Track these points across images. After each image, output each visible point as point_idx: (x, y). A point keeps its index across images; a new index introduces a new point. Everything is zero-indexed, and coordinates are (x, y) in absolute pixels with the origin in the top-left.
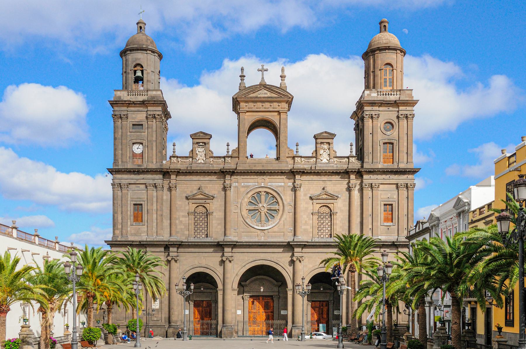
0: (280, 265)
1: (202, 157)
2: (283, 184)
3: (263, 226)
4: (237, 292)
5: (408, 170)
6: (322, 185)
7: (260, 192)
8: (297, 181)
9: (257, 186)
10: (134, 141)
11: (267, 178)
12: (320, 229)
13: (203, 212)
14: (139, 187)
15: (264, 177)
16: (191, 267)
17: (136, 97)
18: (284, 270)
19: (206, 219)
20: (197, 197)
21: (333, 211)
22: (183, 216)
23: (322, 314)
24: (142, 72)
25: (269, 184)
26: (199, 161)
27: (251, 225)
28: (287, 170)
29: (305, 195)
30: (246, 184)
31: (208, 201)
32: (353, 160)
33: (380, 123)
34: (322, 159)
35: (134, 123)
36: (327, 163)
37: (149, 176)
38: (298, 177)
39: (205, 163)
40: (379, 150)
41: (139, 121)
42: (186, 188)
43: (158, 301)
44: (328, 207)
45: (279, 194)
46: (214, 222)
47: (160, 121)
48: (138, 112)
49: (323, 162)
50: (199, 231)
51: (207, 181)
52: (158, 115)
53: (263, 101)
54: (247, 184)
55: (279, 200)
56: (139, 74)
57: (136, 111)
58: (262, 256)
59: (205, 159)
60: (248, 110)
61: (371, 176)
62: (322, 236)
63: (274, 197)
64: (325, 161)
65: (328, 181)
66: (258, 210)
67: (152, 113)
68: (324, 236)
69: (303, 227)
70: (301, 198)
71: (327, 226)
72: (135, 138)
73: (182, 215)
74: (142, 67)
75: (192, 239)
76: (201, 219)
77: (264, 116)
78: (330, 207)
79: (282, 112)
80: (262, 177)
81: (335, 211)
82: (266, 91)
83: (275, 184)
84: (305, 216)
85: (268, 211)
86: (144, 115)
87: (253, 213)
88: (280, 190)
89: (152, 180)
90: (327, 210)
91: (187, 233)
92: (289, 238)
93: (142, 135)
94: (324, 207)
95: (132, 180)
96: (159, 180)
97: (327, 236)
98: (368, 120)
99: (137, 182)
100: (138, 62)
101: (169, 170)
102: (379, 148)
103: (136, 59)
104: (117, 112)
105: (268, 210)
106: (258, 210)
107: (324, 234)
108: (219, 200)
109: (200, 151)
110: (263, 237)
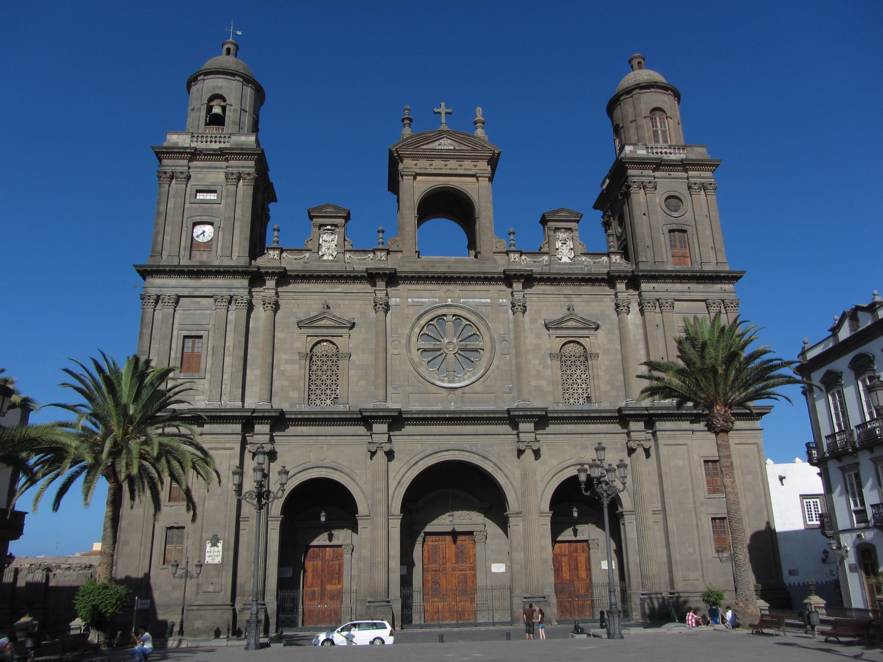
0: (491, 461)
1: (330, 251)
2: (489, 301)
3: (453, 382)
4: (400, 521)
5: (722, 274)
6: (563, 302)
7: (445, 315)
8: (517, 293)
9: (438, 305)
10: (197, 219)
11: (455, 289)
12: (566, 386)
13: (330, 355)
14: (199, 303)
15: (452, 287)
16: (300, 468)
17: (208, 145)
18: (500, 472)
19: (334, 368)
20: (319, 323)
21: (589, 352)
22: (288, 362)
23: (577, 568)
24: (224, 109)
25: (462, 300)
26: (325, 258)
27: (428, 378)
28: (497, 273)
29: (533, 321)
30: (416, 300)
31: (340, 331)
32: (616, 258)
33: (658, 198)
34: (560, 257)
35: (201, 188)
36: (570, 264)
37: (220, 281)
38: (517, 286)
39: (337, 261)
40: (663, 242)
41: (210, 184)
42: (296, 306)
43: (220, 545)
44: (578, 343)
45: (482, 319)
46: (352, 372)
47: (249, 184)
48: (212, 170)
49: (562, 261)
50: (318, 392)
51: (337, 294)
52: (249, 174)
53: (445, 157)
54: (419, 300)
55: (483, 329)
56: (217, 110)
57: (205, 168)
58: (453, 441)
59: (336, 253)
60: (418, 171)
61: (656, 285)
62: (572, 401)
63: (471, 324)
64: (565, 259)
65: (575, 296)
66: (439, 350)
67: (236, 170)
68: (576, 401)
69: (533, 383)
70: (527, 326)
71: (579, 381)
72: (200, 214)
73: (286, 360)
74: (224, 100)
75: (304, 408)
76: (325, 368)
77: (450, 183)
78: (583, 343)
79: (480, 177)
80: (445, 287)
81: (593, 351)
82: (449, 141)
83: (474, 300)
84: (535, 362)
85: (459, 352)
86: (222, 176)
87: (430, 356)
88: (484, 311)
89: (225, 290)
90: (577, 349)
91: (294, 395)
92: (507, 403)
93: (214, 209)
94: (572, 344)
95: (185, 289)
96: (242, 290)
97: (581, 401)
98: (637, 192)
99: (196, 294)
100: (217, 92)
101: (263, 271)
102: (663, 239)
103: (214, 88)
104: (167, 168)
105: (461, 350)
106: (439, 350)
107: (576, 396)
108: (363, 331)
109: (327, 239)
110: (453, 404)
